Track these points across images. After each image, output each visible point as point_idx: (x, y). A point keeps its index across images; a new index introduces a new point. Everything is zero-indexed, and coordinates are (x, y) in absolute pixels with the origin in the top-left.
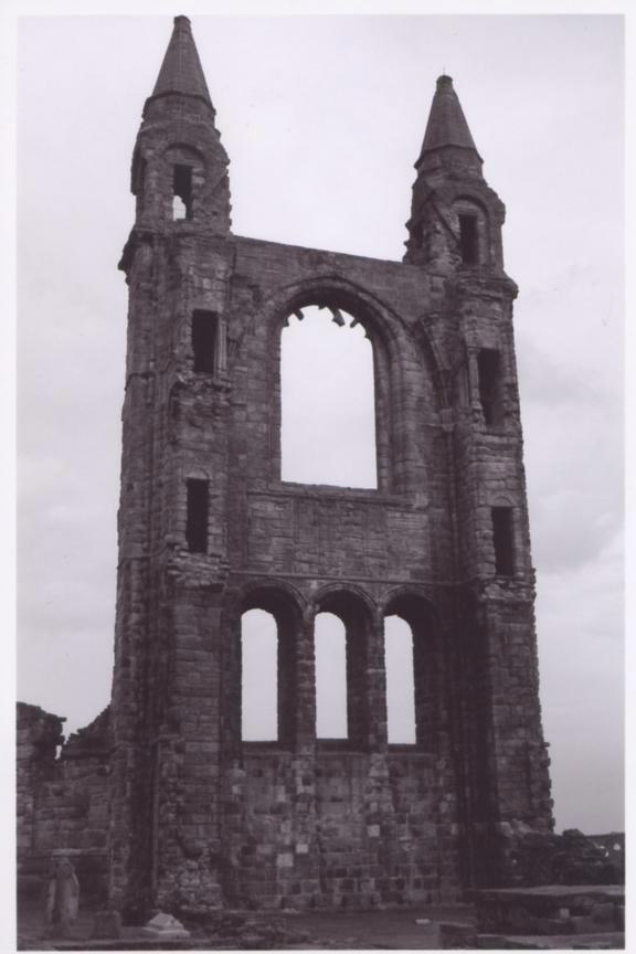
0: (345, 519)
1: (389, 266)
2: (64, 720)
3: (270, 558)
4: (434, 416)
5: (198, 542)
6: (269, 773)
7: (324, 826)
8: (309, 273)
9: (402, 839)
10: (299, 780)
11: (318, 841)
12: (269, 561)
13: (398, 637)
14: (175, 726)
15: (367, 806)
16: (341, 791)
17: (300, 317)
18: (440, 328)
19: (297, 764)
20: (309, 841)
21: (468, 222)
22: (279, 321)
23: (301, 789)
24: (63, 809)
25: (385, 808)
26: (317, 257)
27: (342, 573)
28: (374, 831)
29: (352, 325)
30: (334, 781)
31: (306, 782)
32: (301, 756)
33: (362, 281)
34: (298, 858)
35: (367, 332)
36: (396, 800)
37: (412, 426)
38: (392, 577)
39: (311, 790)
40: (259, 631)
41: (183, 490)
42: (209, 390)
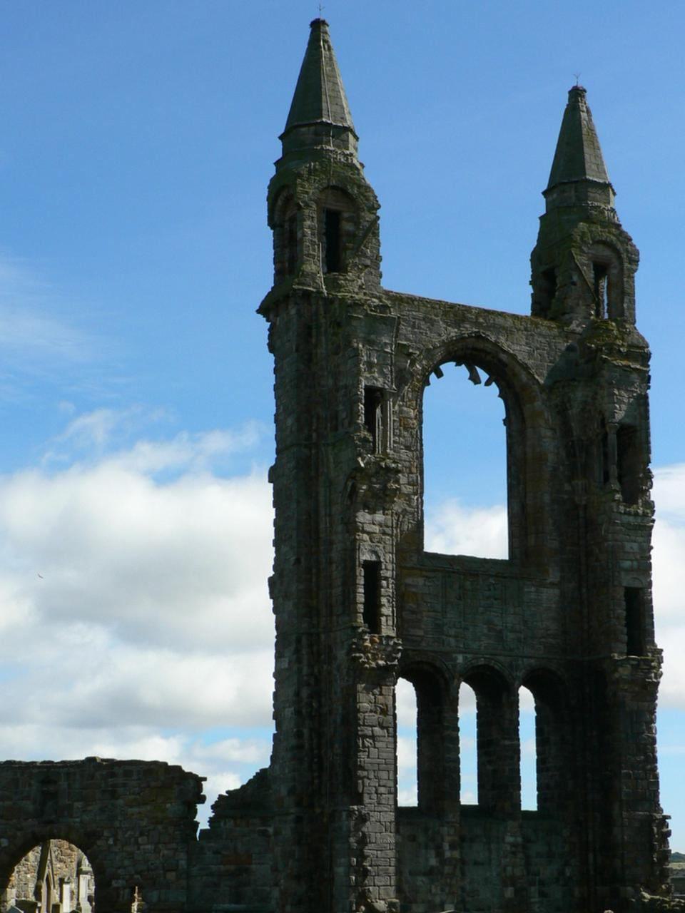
0: (487, 593)
2: (205, 779)
3: (421, 633)
4: (567, 487)
6: (421, 839)
7: (468, 888)
8: (454, 332)
9: (533, 900)
10: (446, 846)
11: (463, 901)
14: (359, 799)
15: (505, 870)
17: (439, 374)
20: (455, 901)
23: (448, 854)
24: (222, 867)
25: (518, 872)
28: (509, 893)
29: (488, 383)
31: (452, 847)
32: (448, 823)
35: (500, 393)
36: (528, 864)
37: (547, 498)
39: (456, 854)
41: (361, 572)
42: (382, 472)
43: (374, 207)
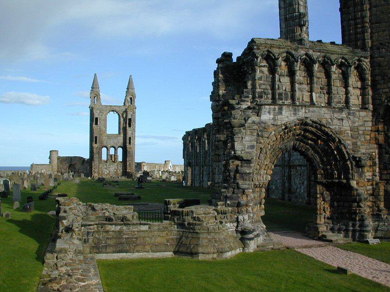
1: (120, 107)
5: (96, 143)
12: (105, 143)
13: (120, 151)
21: (131, 98)
22: (107, 114)
26: (111, 106)
27: (112, 144)
40: (104, 150)
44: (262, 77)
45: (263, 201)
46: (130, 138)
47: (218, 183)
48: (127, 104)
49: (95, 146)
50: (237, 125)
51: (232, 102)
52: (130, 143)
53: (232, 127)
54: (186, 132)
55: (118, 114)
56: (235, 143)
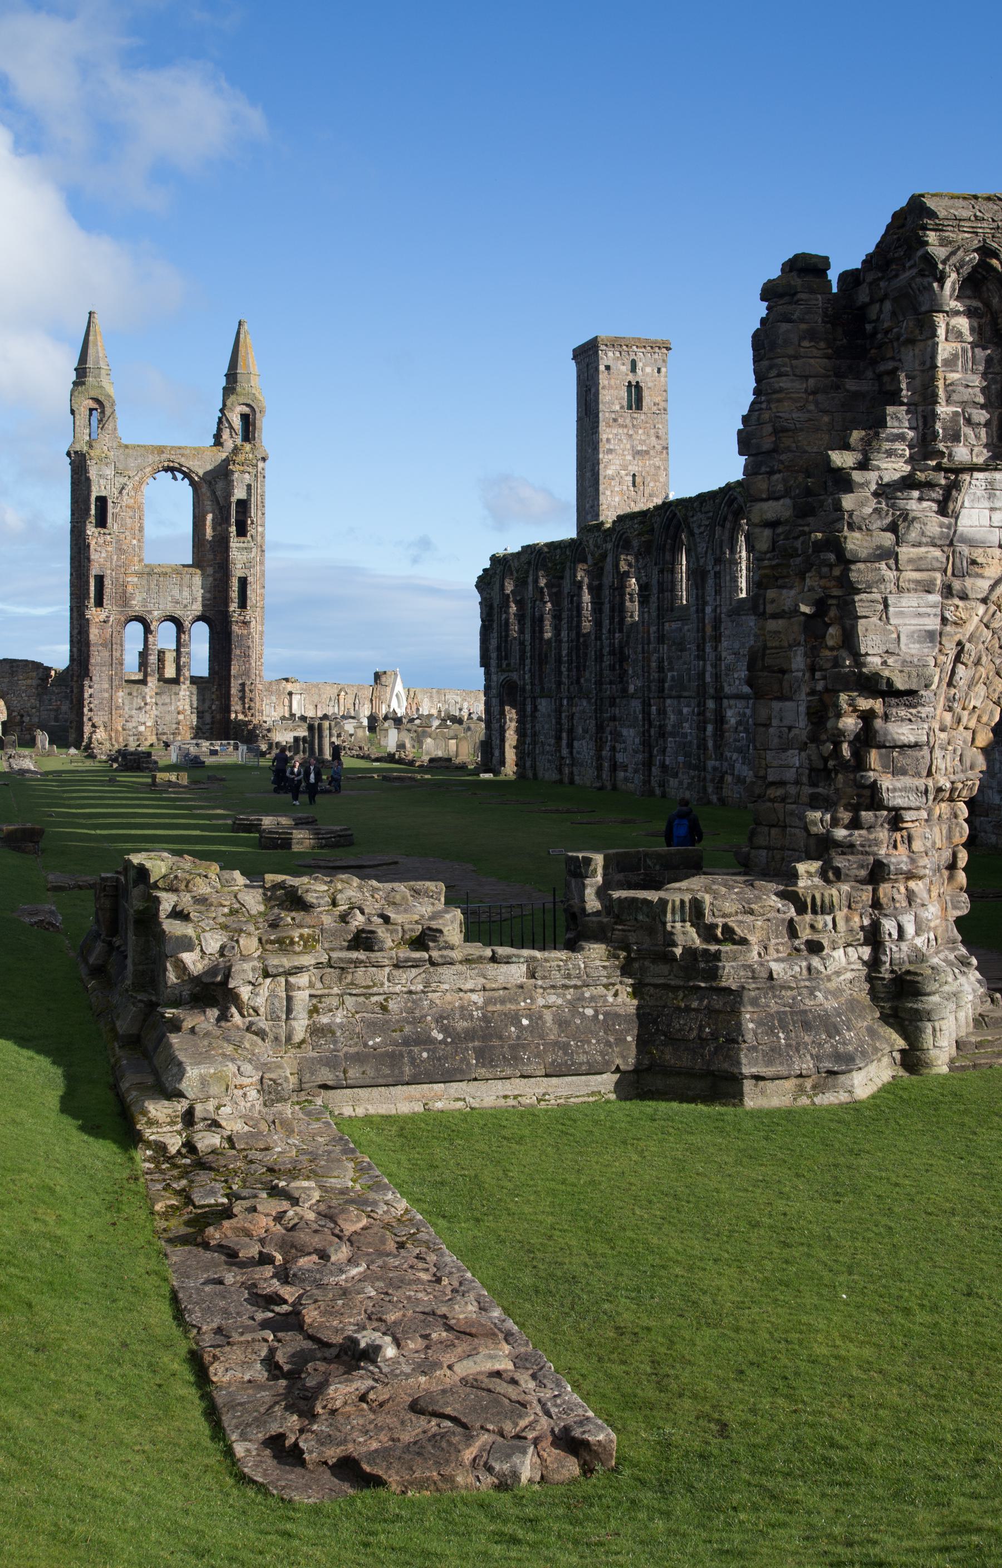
5: (99, 603)
6: (135, 694)
12: (137, 605)
14: (91, 680)
16: (168, 700)
18: (220, 485)
19: (147, 690)
21: (245, 418)
23: (148, 700)
26: (161, 450)
29: (183, 479)
30: (164, 697)
33: (183, 461)
34: (146, 727)
38: (194, 607)
43: (113, 404)
44: (955, 356)
45: (963, 858)
46: (243, 582)
47: (782, 783)
48: (229, 444)
49: (94, 614)
50: (863, 554)
51: (842, 459)
52: (243, 604)
53: (845, 561)
54: (494, 559)
55: (192, 483)
56: (861, 621)
